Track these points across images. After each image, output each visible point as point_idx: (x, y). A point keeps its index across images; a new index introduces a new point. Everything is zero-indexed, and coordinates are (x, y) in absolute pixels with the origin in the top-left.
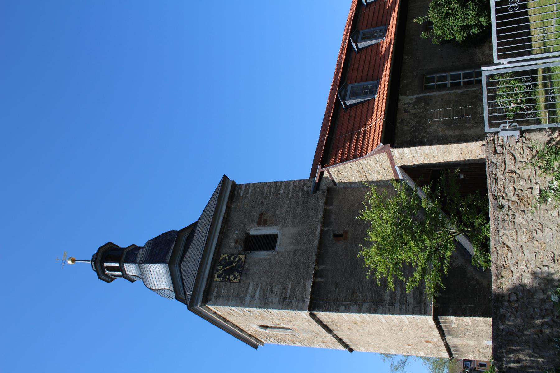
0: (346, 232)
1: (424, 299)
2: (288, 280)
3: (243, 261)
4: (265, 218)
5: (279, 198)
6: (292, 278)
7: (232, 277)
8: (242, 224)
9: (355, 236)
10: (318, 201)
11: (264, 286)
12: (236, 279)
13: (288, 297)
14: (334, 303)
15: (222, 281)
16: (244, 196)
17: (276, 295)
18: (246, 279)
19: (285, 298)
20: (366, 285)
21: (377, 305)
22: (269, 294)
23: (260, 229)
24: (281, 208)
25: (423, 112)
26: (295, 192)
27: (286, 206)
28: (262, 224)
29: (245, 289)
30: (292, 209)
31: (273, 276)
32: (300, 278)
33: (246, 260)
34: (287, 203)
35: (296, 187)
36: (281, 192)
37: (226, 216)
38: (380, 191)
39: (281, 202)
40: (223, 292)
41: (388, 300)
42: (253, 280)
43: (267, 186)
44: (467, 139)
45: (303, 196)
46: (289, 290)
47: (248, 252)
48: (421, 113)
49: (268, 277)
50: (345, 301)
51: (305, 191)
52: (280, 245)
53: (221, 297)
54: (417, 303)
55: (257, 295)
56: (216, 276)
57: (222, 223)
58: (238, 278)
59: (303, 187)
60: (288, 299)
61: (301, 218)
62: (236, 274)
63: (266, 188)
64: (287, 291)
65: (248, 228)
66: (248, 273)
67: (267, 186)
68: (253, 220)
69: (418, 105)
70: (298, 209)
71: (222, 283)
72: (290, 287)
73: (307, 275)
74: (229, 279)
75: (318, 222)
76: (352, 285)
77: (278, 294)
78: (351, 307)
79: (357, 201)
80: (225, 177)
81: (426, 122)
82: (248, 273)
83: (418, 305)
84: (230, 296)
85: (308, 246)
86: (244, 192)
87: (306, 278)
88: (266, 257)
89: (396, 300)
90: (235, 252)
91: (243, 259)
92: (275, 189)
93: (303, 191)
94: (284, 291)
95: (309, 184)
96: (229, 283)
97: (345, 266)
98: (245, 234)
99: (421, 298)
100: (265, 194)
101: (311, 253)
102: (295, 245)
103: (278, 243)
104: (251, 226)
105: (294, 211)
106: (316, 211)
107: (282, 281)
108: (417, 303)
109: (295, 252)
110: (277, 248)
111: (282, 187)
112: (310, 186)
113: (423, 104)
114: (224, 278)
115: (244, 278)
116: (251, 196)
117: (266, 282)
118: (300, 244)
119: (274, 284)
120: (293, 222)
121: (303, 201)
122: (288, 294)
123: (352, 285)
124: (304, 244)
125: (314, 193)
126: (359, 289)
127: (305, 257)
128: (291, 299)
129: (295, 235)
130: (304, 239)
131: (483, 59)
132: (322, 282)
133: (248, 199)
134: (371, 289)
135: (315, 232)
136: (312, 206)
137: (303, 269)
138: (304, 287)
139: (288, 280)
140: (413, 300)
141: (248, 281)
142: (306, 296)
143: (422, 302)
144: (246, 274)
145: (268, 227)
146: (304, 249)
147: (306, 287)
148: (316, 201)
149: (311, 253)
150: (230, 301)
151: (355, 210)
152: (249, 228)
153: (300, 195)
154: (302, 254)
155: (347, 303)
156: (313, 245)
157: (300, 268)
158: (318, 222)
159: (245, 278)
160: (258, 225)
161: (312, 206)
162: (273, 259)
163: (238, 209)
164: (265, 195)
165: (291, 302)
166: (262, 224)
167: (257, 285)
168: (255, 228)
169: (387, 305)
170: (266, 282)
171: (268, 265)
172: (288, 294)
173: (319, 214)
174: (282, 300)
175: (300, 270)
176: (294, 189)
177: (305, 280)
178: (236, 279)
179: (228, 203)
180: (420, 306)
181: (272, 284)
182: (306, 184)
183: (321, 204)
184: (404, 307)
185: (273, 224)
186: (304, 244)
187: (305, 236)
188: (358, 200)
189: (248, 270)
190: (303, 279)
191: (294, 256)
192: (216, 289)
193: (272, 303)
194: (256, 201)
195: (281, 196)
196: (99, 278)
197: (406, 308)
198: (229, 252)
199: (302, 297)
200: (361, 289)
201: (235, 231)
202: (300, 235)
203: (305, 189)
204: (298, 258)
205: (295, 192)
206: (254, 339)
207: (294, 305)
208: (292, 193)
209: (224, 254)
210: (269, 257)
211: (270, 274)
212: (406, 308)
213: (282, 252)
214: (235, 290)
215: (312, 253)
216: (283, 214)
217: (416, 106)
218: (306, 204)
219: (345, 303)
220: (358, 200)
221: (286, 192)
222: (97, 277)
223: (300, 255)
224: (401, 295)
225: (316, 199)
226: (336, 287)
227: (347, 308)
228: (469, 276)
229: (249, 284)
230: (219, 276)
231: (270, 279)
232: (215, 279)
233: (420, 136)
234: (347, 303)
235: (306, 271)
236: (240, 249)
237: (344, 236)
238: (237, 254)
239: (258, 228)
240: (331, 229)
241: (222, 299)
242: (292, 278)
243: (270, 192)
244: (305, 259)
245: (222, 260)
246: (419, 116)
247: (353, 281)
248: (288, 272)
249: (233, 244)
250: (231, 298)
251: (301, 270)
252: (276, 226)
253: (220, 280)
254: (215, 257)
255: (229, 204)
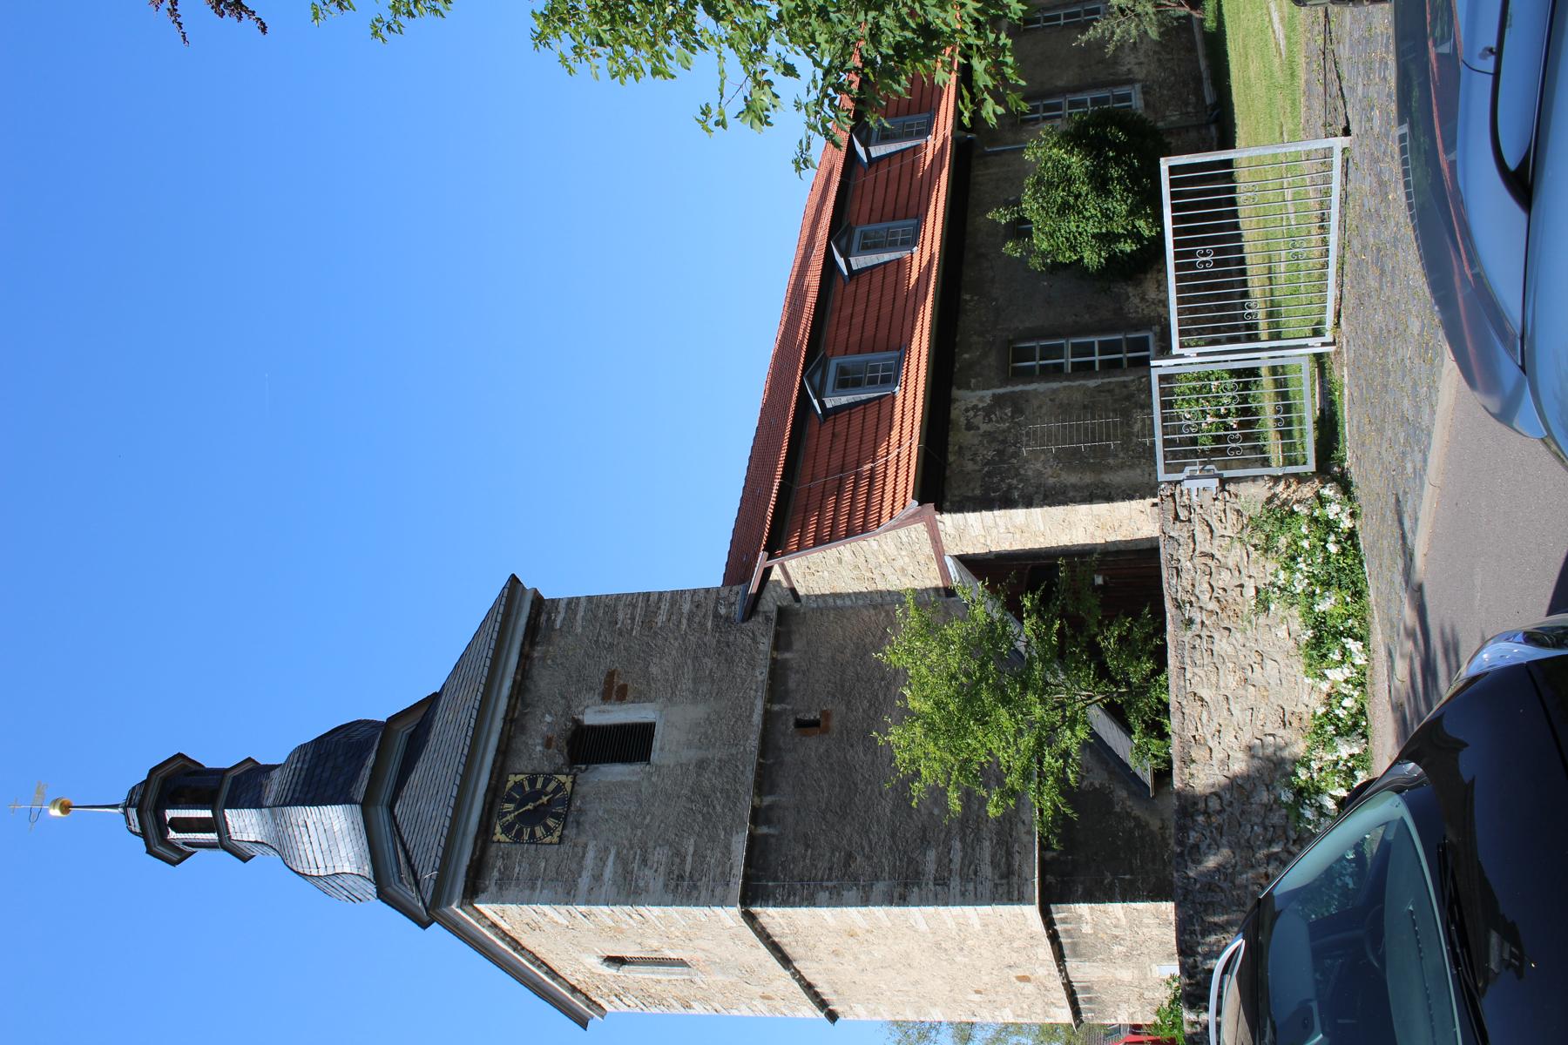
0: (826, 715)
1: (1016, 867)
2: (686, 835)
3: (569, 789)
4: (621, 682)
5: (655, 633)
6: (697, 828)
8: (563, 697)
9: (849, 725)
10: (754, 639)
11: (625, 851)
12: (551, 834)
13: (687, 874)
14: (802, 885)
15: (515, 842)
16: (565, 629)
17: (656, 871)
18: (578, 834)
19: (681, 877)
20: (879, 839)
21: (906, 885)
22: (639, 868)
23: (608, 711)
24: (661, 658)
25: (1009, 428)
26: (697, 620)
27: (674, 652)
29: (577, 859)
30: (689, 661)
31: (647, 826)
32: (714, 827)
33: (576, 788)
34: (676, 644)
35: (697, 607)
36: (661, 618)
37: (519, 677)
39: (660, 642)
40: (517, 870)
42: (595, 837)
45: (717, 627)
46: (689, 859)
47: (580, 769)
48: (1004, 431)
49: (635, 827)
50: (829, 879)
51: (721, 617)
52: (662, 749)
53: (514, 882)
54: (1001, 877)
55: (608, 873)
56: (498, 829)
57: (510, 697)
58: (558, 833)
59: (716, 608)
60: (687, 879)
61: (713, 681)
62: (551, 822)
63: (620, 607)
64: (683, 860)
66: (582, 819)
70: (706, 660)
71: (514, 846)
72: (691, 850)
73: (733, 820)
74: (532, 835)
75: (756, 691)
76: (845, 842)
77: (662, 869)
78: (845, 893)
80: (514, 580)
81: (1016, 455)
83: (1004, 881)
84: (537, 879)
86: (564, 619)
87: (731, 828)
88: (628, 778)
89: (951, 871)
90: (546, 769)
91: (568, 786)
92: (646, 611)
93: (716, 615)
94: (677, 860)
95: (733, 600)
96: (534, 846)
98: (569, 724)
99: (1009, 865)
101: (741, 768)
103: (656, 744)
104: (585, 704)
105: (694, 666)
106: (752, 664)
108: (1001, 877)
109: (701, 765)
110: (654, 757)
111: (663, 607)
113: (1008, 411)
114: (519, 834)
115: (571, 832)
116: (583, 627)
117: (631, 840)
119: (651, 844)
120: (695, 693)
121: (718, 642)
122: (688, 868)
123: (845, 842)
126: (863, 849)
127: (727, 777)
128: (695, 878)
130: (722, 733)
131: (1143, 310)
132: (773, 836)
133: (577, 635)
134: (890, 848)
135: (750, 716)
136: (740, 653)
137: (724, 806)
138: (727, 848)
139: (686, 835)
140: (990, 869)
142: (734, 872)
144: (578, 823)
145: (630, 705)
147: (733, 848)
148: (749, 641)
149: (741, 768)
150: (538, 891)
152: (580, 709)
153: (709, 624)
154: (720, 768)
155: (834, 883)
156: (745, 749)
158: (756, 691)
159: (575, 831)
161: (740, 653)
162: (645, 784)
163: (549, 662)
164: (618, 626)
165: (695, 887)
167: (607, 849)
168: (597, 708)
169: (931, 883)
170: (631, 840)
172: (688, 868)
174: (672, 884)
175: (714, 807)
177: (729, 832)
178: (551, 834)
179: (523, 645)
180: (1008, 883)
181: (646, 843)
183: (761, 647)
184: (971, 887)
185: (642, 698)
187: (724, 727)
189: (580, 811)
190: (725, 829)
191: (698, 775)
192: (499, 863)
193: (647, 892)
194: (597, 641)
195: (660, 628)
196: (150, 851)
197: (976, 888)
199: (723, 873)
201: (543, 716)
202: (711, 723)
203: (723, 611)
204: (709, 779)
205: (697, 620)
206: (583, 998)
207: (704, 893)
208: (688, 620)
209: (516, 774)
210: (635, 779)
212: (976, 888)
214: (551, 862)
215: (745, 767)
216: (666, 673)
217: (993, 416)
219: (830, 884)
222: (144, 849)
223: (714, 773)
224: (963, 859)
226: (807, 846)
227: (835, 897)
228: (1118, 809)
229: (585, 846)
230: (507, 829)
231: (639, 832)
232: (495, 838)
233: (1004, 487)
234: (834, 883)
235: (730, 809)
236: (560, 760)
237: (822, 725)
239: (603, 707)
240: (789, 707)
241: (517, 885)
242: (697, 828)
243: (633, 619)
244: (727, 782)
245: (512, 788)
246: (1001, 438)
247: (848, 830)
249: (539, 748)
250: (539, 883)
253: (508, 840)
254: (493, 782)
255: (527, 648)
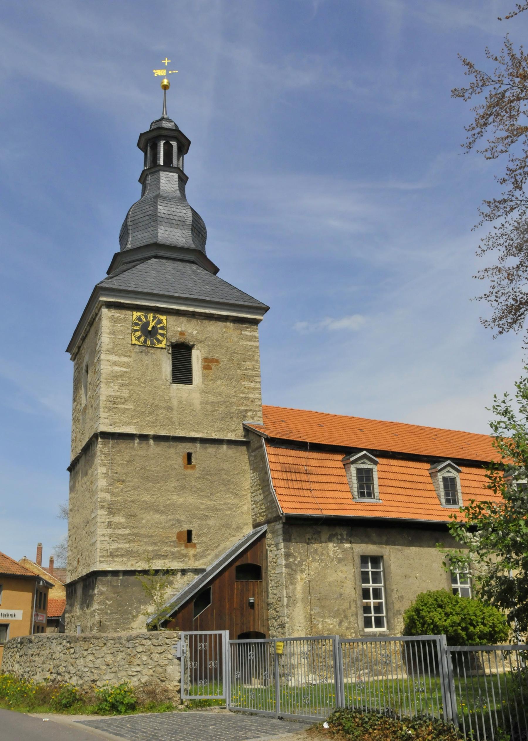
0: (194, 467)
1: (116, 559)
2: (135, 404)
3: (158, 346)
4: (213, 367)
5: (238, 381)
6: (138, 409)
7: (138, 334)
8: (205, 339)
9: (188, 479)
10: (234, 430)
11: (127, 375)
12: (136, 340)
13: (116, 406)
14: (109, 460)
15: (132, 323)
16: (242, 336)
17: (118, 391)
18: (136, 353)
19: (114, 403)
20: (131, 495)
21: (108, 508)
22: (119, 383)
23: (198, 362)
24: (225, 385)
25: (330, 556)
26: (245, 402)
27: (228, 392)
28: (206, 364)
29: (124, 353)
30: (223, 399)
31: (140, 385)
32: (139, 417)
33: (159, 349)
34: (232, 392)
35: (252, 401)
36: (246, 384)
37: (216, 316)
38: (243, 505)
39: (233, 384)
40: (119, 325)
41: (114, 521)
42: (134, 361)
43: (255, 364)
44: (290, 606)
45: (241, 412)
46: (123, 406)
47: (169, 350)
48: (328, 554)
49: (139, 379)
50: (112, 472)
51: (246, 413)
52: (178, 389)
53: (112, 324)
54: (111, 553)
55: (117, 369)
56: (139, 314)
57: (205, 313)
58: (137, 343)
59: (251, 410)
60: (113, 406)
61: (212, 412)
62: (143, 339)
63: (253, 363)
64: (123, 403)
65: (201, 346)
66: (144, 354)
67: (255, 364)
68: (210, 352)
69: (339, 550)
70: (223, 407)
71: (131, 322)
72: (127, 407)
73: (142, 426)
74: (136, 331)
75: (207, 433)
76: (130, 479)
77: (118, 394)
78: (105, 480)
79: (232, 478)
80: (264, 309)
81: (314, 560)
82: (144, 354)
83: (109, 554)
84: (114, 335)
85: (177, 424)
86: (247, 335)
87: (138, 425)
88: (164, 374)
89: (115, 529)
90: (169, 335)
91: (160, 346)
92: (250, 376)
93: (247, 411)
94: (123, 401)
95: (255, 418)
96: (130, 332)
97: (153, 469)
98: (192, 343)
99: (117, 556)
100: (244, 363)
101: (168, 428)
102: (178, 408)
103: (181, 386)
104: (202, 350)
105: (221, 402)
106: (221, 430)
107: (135, 396)
108: (111, 553)
109: (170, 409)
110: (175, 385)
111: (252, 384)
112: (253, 419)
113: (340, 556)
114: (137, 324)
115: (137, 349)
116: (242, 345)
117: (133, 378)
118: (180, 414)
119: (131, 388)
120: (207, 403)
121: (233, 413)
122: (119, 406)
123: (130, 479)
124: (180, 419)
125: (243, 424)
126: (126, 488)
127: (163, 422)
128: (114, 410)
129: (190, 406)
130: (185, 418)
131: (399, 626)
132: (134, 445)
133: (238, 342)
134: (126, 501)
135: (194, 431)
136: (227, 424)
137: (149, 421)
138: (127, 424)
139: (135, 404)
140: (115, 547)
141: (133, 355)
142: (117, 428)
143: (112, 558)
144: (141, 352)
145: (201, 372)
146: (173, 419)
147: (128, 427)
148: (233, 428)
149: (168, 428)
150: (108, 336)
151: (220, 477)
152: (200, 348)
153: (242, 408)
154: (168, 418)
155: (110, 475)
156: (177, 429)
157: (151, 417)
158: (207, 433)
159: (138, 351)
160: (204, 358)
161: (227, 424)
162: (161, 382)
163: (224, 330)
164: (243, 363)
165: (110, 410)
166: (206, 364)
167: (129, 367)
168: (200, 356)
169: (109, 520)
170: (133, 378)
171: (153, 378)
172: (119, 406)
173: (216, 433)
174: (110, 399)
175: (148, 416)
176: (250, 400)
177: (136, 424)
178: (136, 340)
179: (233, 317)
180: (108, 556)
181: (131, 385)
182: (256, 414)
183: (230, 434)
184: (107, 538)
185: (205, 377)
186: (180, 419)
187: (189, 419)
188: (233, 480)
189: (147, 353)
190: (137, 422)
191: (164, 408)
192: (122, 316)
193: (108, 388)
194: (234, 353)
195: (241, 384)
197: (106, 541)
198: (169, 326)
199: (116, 423)
200: (126, 489)
201: (196, 330)
202: (191, 412)
203: (249, 414)
204: (162, 413)
205: (245, 402)
207: (107, 414)
208: (245, 397)
209: (166, 320)
210: (163, 377)
211: (143, 381)
212: (106, 541)
213: (169, 393)
214: (123, 341)
215: (168, 430)
216: (217, 389)
217: (337, 548)
218: (229, 417)
219: (110, 473)
220: (233, 480)
221: (246, 390)
222: (142, 132)
223: (165, 415)
224: (120, 534)
225: (237, 428)
226: (128, 462)
227: (104, 475)
228: (142, 607)
229: (130, 356)
230: (139, 319)
231: (136, 382)
232: (134, 313)
233: (296, 554)
234: (110, 475)
235: (147, 424)
236: (174, 340)
237: (189, 466)
238: (166, 336)
239: (200, 359)
240: (198, 450)
241: (111, 326)
242: (138, 409)
243: (246, 370)
244: (160, 422)
245: (159, 319)
246: (324, 552)
247: (136, 480)
248: (145, 403)
249: (180, 329)
250: (112, 336)
251: (148, 419)
252: (203, 382)
253: (133, 319)
254: (162, 309)
255: (231, 318)
